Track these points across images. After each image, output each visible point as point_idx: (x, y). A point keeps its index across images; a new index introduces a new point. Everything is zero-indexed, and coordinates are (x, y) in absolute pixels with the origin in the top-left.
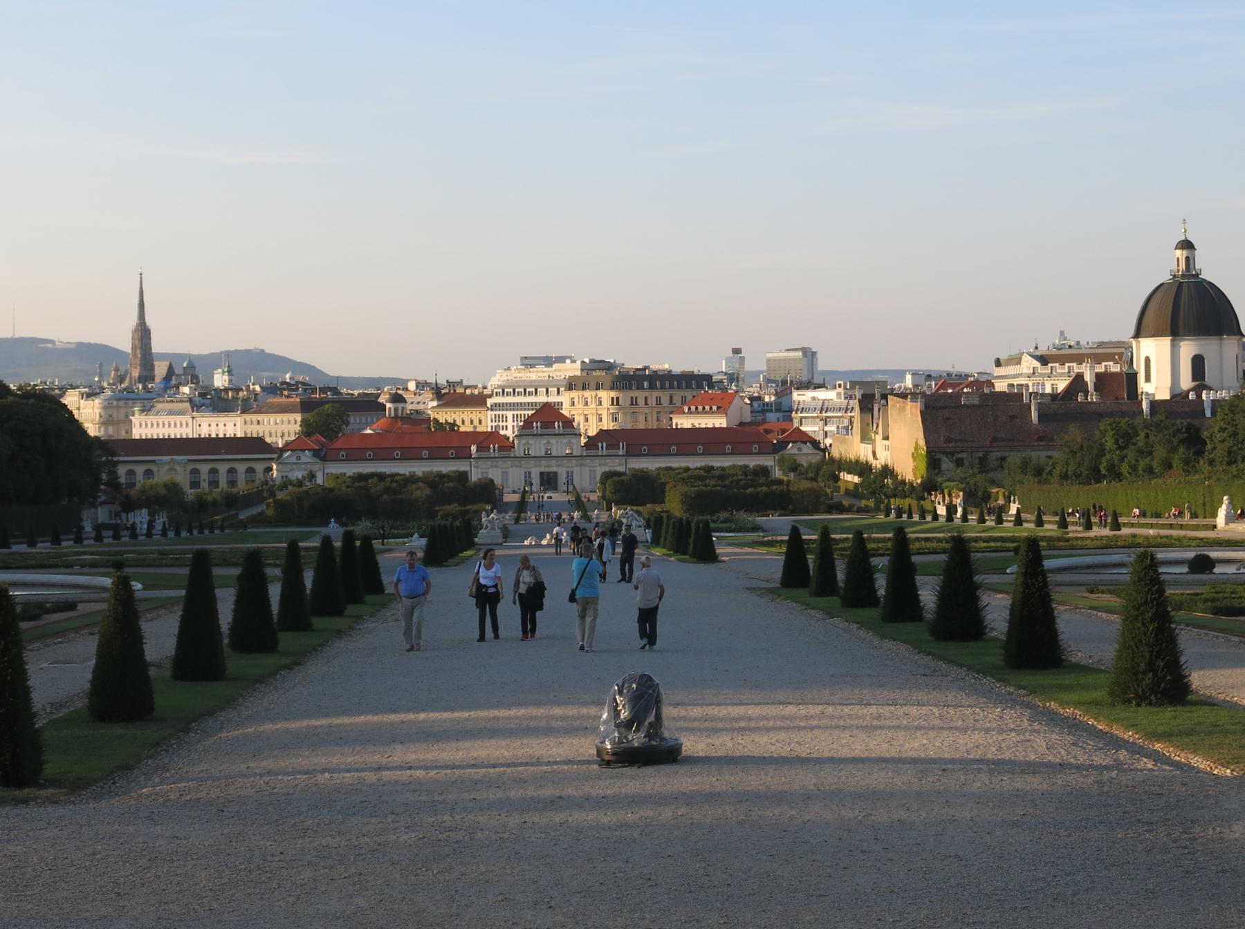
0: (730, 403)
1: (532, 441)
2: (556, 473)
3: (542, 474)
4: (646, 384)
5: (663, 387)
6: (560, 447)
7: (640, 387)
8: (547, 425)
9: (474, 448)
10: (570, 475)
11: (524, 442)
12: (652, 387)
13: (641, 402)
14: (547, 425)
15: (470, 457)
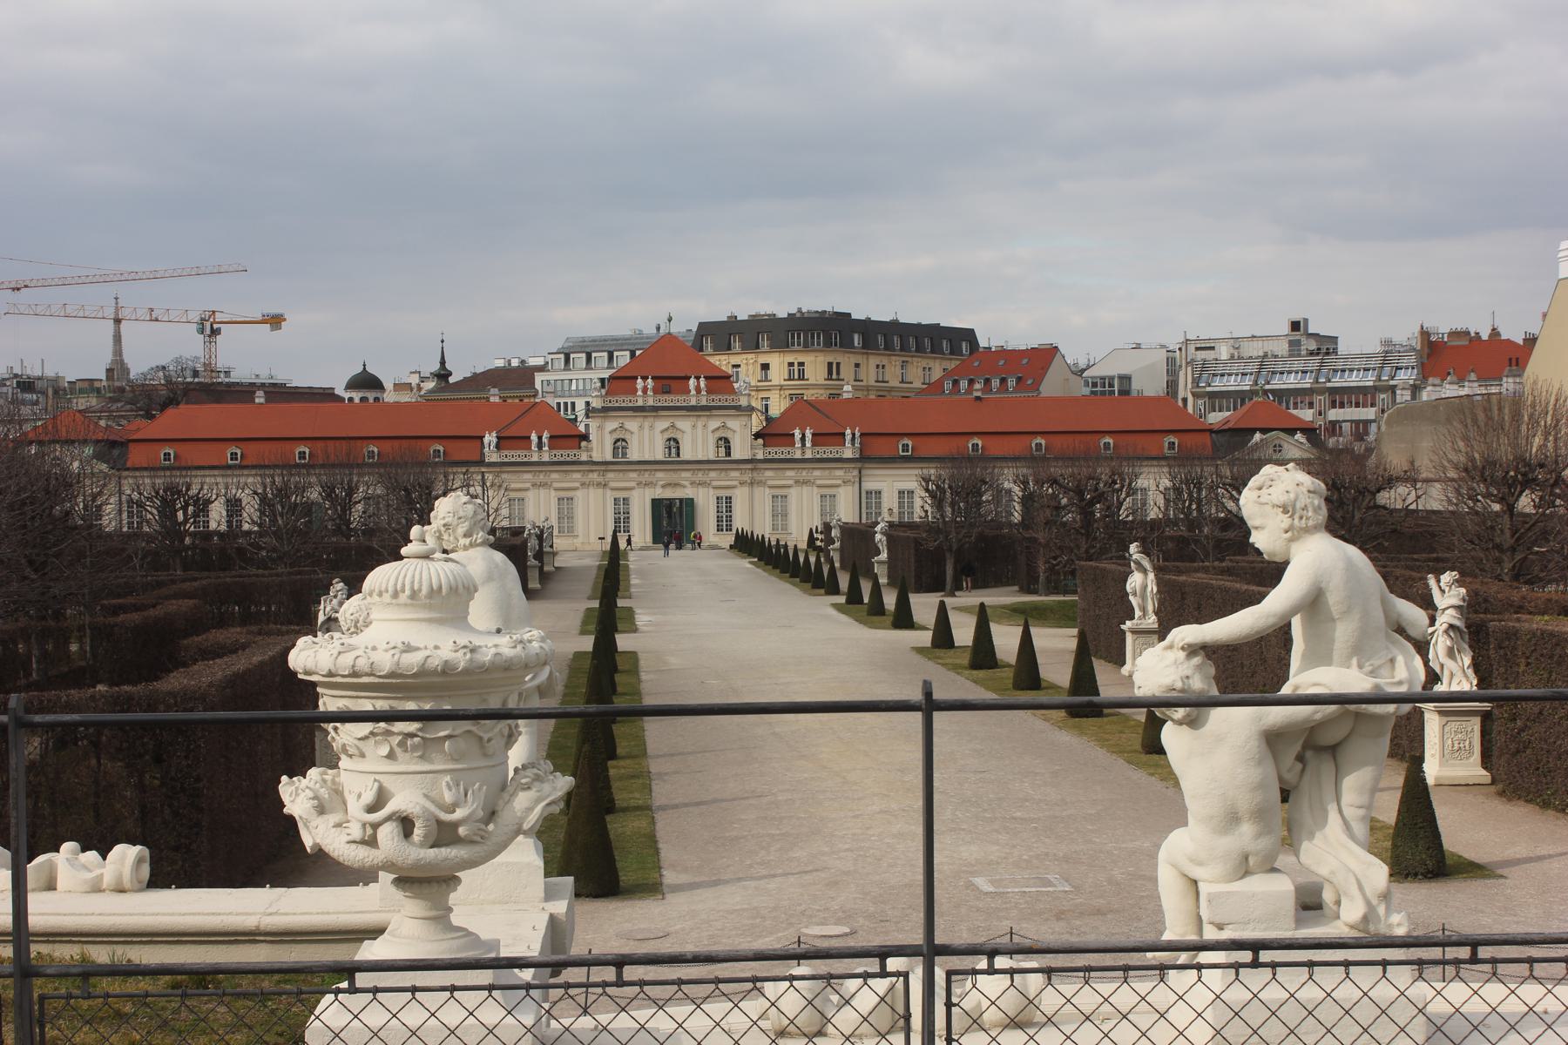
0: (1045, 369)
1: (632, 425)
2: (690, 503)
3: (656, 503)
4: (856, 338)
5: (888, 347)
6: (697, 440)
7: (846, 345)
8: (669, 383)
9: (490, 438)
10: (725, 506)
11: (611, 425)
12: (868, 345)
13: (847, 372)
14: (669, 383)
15: (481, 462)
